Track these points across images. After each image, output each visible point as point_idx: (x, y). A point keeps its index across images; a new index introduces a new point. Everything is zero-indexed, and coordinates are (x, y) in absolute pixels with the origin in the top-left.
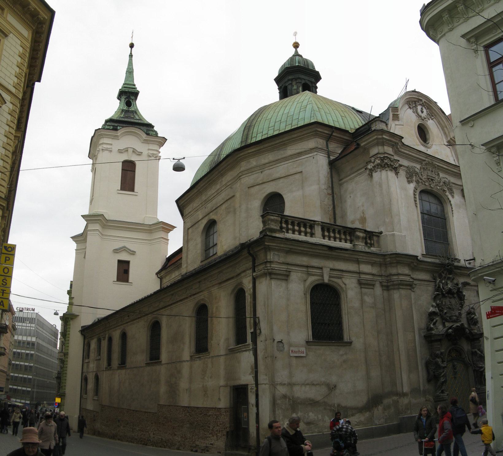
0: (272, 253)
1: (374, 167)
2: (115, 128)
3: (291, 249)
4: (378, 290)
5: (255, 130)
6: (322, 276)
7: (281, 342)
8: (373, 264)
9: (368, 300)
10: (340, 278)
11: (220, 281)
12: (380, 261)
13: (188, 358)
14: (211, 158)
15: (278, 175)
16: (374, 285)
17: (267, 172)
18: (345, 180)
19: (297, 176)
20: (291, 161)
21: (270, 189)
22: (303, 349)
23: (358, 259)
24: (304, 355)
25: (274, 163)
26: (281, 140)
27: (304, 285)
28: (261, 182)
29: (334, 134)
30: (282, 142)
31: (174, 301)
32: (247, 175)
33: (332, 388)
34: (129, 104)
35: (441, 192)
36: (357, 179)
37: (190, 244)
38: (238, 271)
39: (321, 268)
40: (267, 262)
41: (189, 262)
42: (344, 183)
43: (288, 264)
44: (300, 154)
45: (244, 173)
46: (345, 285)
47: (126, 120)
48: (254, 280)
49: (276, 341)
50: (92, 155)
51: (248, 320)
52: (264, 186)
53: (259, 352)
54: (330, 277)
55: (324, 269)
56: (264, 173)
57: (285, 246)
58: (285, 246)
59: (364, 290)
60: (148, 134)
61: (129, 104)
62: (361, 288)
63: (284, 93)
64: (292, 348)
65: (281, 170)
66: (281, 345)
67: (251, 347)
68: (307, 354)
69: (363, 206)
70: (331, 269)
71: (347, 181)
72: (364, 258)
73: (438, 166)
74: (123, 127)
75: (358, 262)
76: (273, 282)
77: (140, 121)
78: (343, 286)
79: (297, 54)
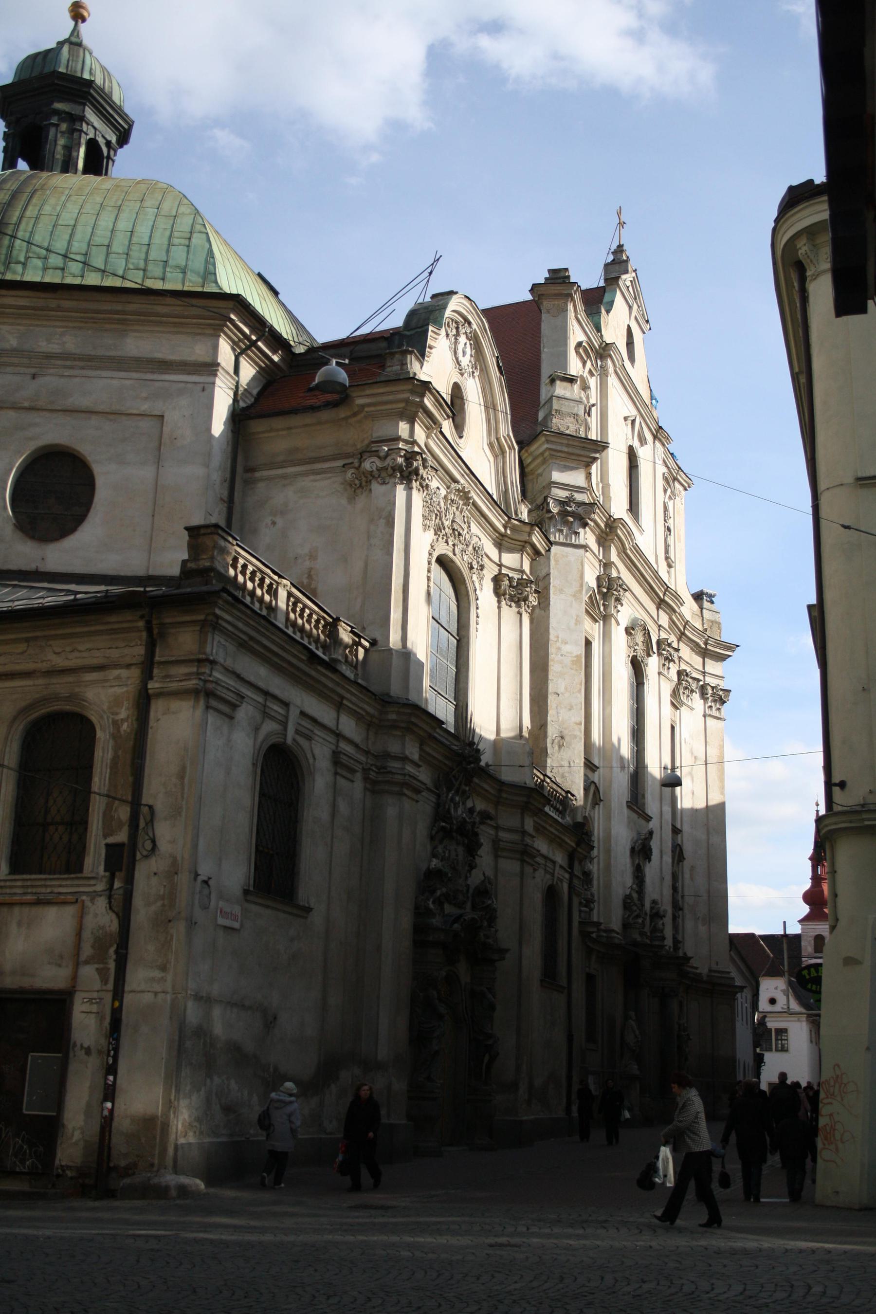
0: (217, 638)
1: (379, 470)
3: (252, 638)
4: (358, 785)
6: (284, 724)
7: (206, 882)
8: (358, 717)
9: (343, 807)
10: (309, 738)
12: (372, 716)
15: (85, 402)
16: (353, 771)
17: (50, 381)
18: (265, 473)
19: (145, 425)
20: (135, 375)
21: (53, 432)
22: (237, 910)
23: (343, 698)
24: (236, 925)
25: (81, 364)
26: (119, 307)
27: (255, 739)
28: (26, 404)
29: (260, 343)
30: (117, 312)
33: (270, 1021)
35: (465, 571)
36: (306, 482)
38: (60, 662)
39: (286, 705)
40: (207, 660)
42: (261, 480)
43: (239, 677)
44: (165, 366)
46: (315, 759)
48: (144, 702)
49: (200, 878)
51: (97, 807)
52: (35, 417)
53: (138, 901)
54: (297, 732)
55: (292, 708)
56: (41, 380)
57: (245, 628)
58: (245, 628)
59: (341, 781)
62: (336, 773)
64: (221, 904)
65: (99, 388)
66: (206, 891)
67: (100, 887)
68: (242, 925)
69: (312, 556)
70: (303, 714)
71: (270, 479)
72: (354, 699)
73: (475, 504)
75: (339, 706)
76: (212, 717)
78: (311, 761)
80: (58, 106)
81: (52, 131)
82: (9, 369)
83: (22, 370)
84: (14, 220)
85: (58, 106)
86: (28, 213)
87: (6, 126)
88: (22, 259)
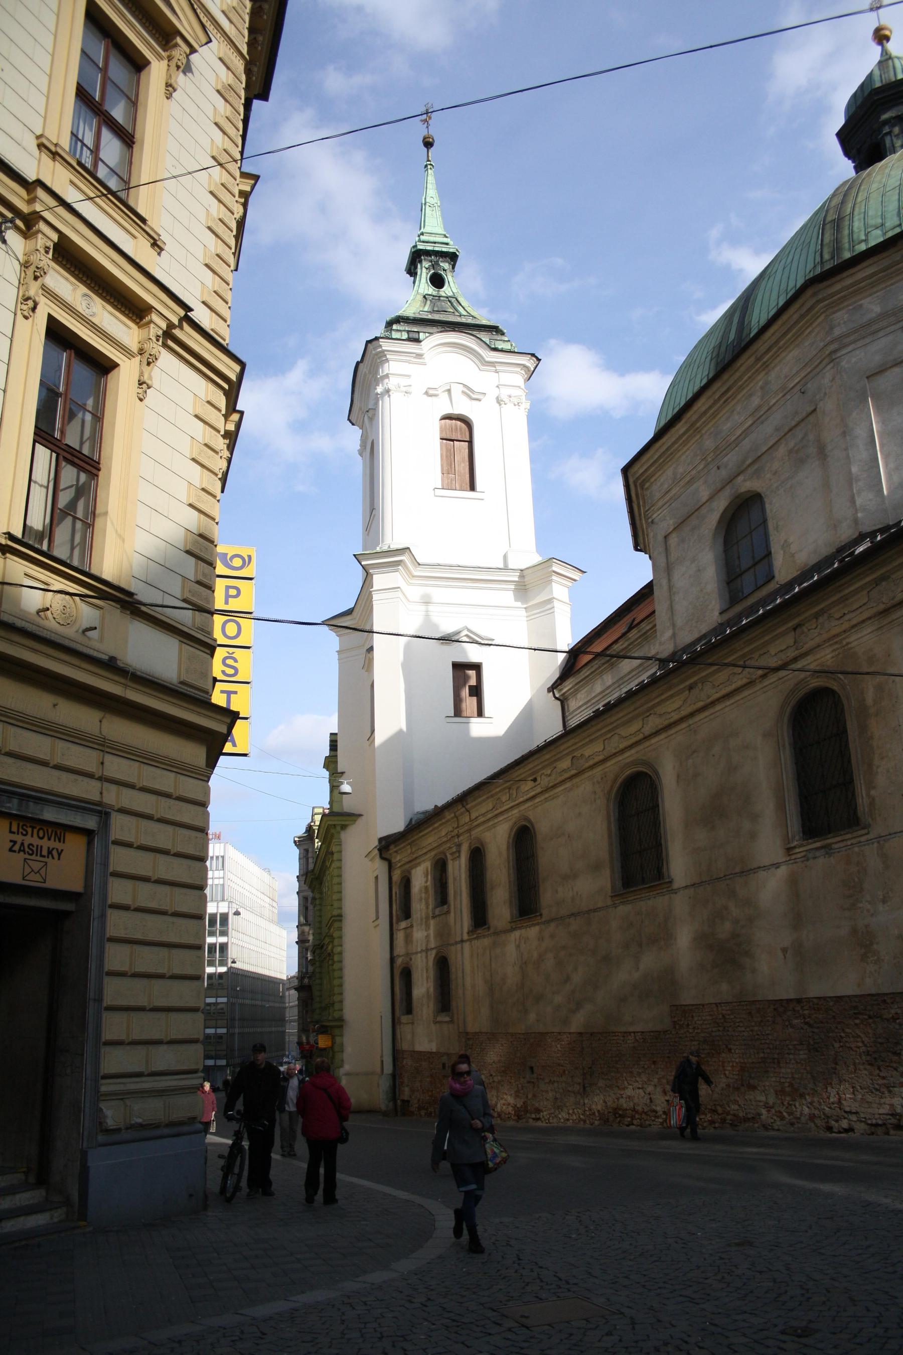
2: (415, 336)
5: (857, 224)
11: (882, 607)
13: (778, 855)
14: (714, 342)
31: (701, 704)
32: (860, 344)
34: (437, 281)
37: (677, 575)
41: (679, 622)
45: (848, 340)
47: (436, 317)
50: (353, 424)
60: (495, 349)
61: (437, 281)
63: (857, 173)
74: (431, 334)
77: (470, 321)
79: (886, 59)
80: (885, 117)
81: (888, 140)
82: (881, 334)
83: (892, 328)
84: (848, 211)
85: (885, 117)
86: (859, 199)
87: (853, 162)
88: (863, 238)
